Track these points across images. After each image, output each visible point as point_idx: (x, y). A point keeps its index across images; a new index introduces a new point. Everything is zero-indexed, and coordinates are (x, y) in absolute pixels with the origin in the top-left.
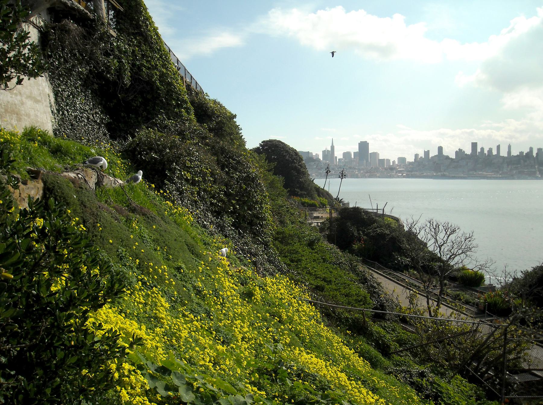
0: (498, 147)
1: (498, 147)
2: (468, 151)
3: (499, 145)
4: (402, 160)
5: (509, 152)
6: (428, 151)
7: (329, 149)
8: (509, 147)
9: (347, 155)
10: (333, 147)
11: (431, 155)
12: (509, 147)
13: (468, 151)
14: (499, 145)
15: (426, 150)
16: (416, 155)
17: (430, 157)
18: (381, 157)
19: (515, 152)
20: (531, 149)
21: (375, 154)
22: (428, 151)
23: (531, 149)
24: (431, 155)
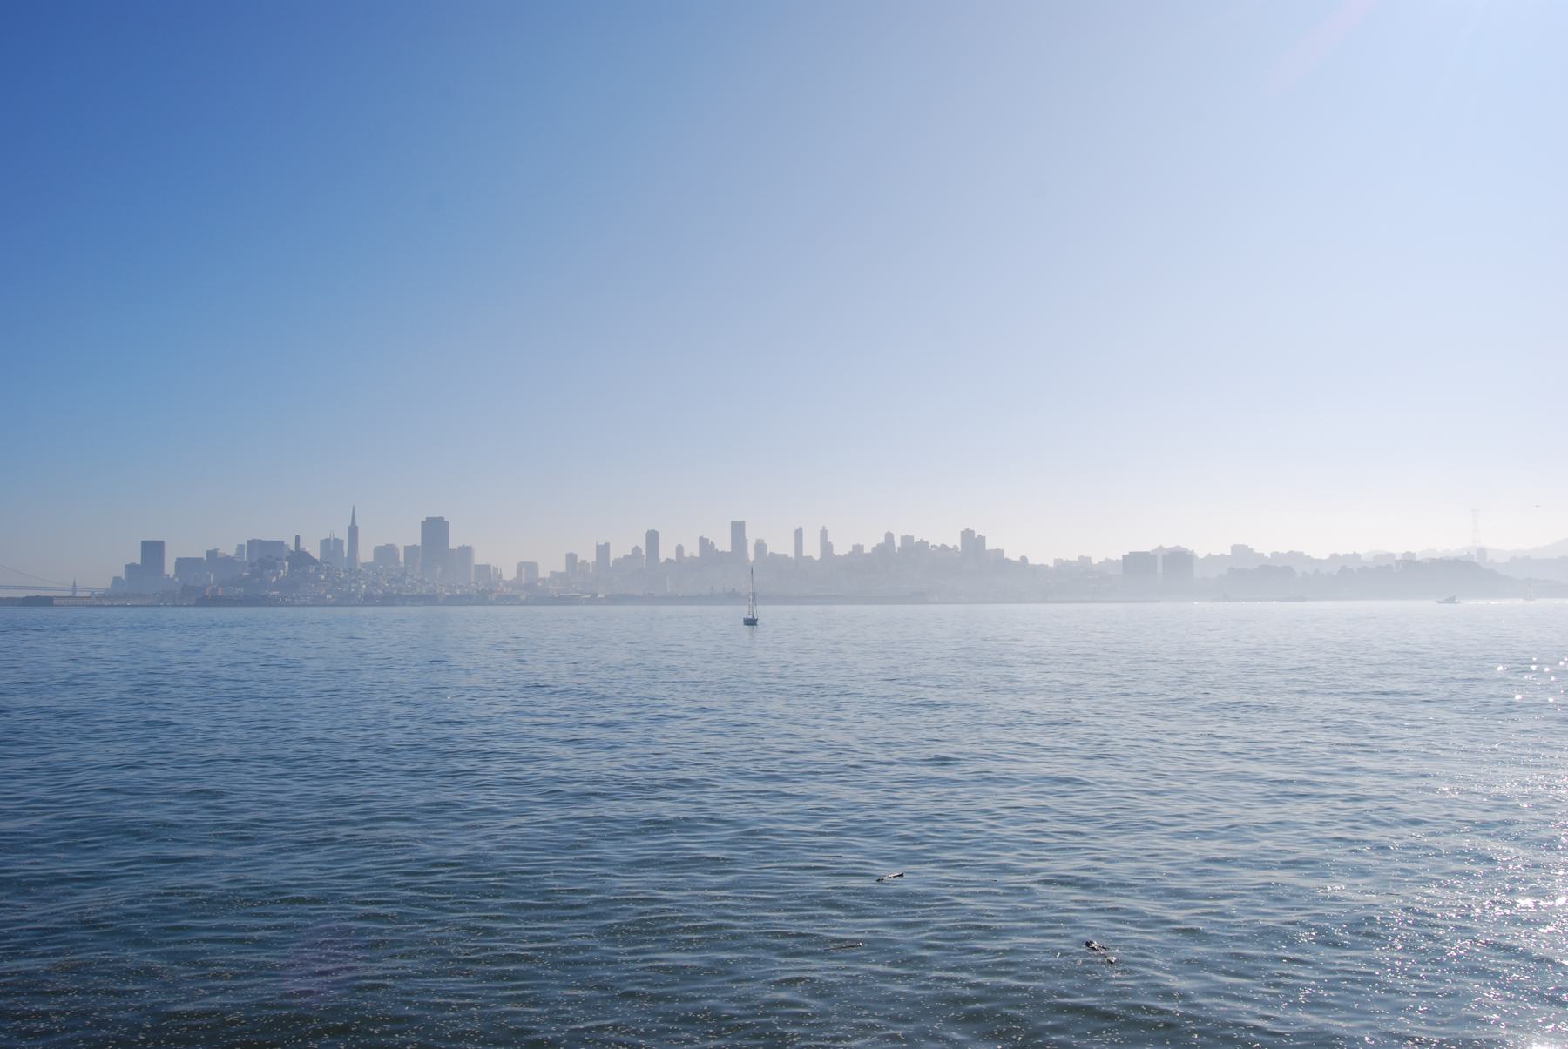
0: (799, 534)
1: (799, 534)
2: (723, 544)
3: (801, 529)
4: (528, 568)
5: (826, 547)
6: (607, 545)
7: (343, 535)
8: (824, 533)
9: (386, 552)
10: (353, 531)
11: (616, 554)
12: (824, 533)
13: (723, 544)
14: (801, 529)
15: (602, 543)
16: (571, 558)
17: (612, 558)
18: (479, 559)
19: (841, 548)
20: (889, 537)
21: (466, 551)
22: (607, 545)
23: (889, 537)
24: (616, 554)
